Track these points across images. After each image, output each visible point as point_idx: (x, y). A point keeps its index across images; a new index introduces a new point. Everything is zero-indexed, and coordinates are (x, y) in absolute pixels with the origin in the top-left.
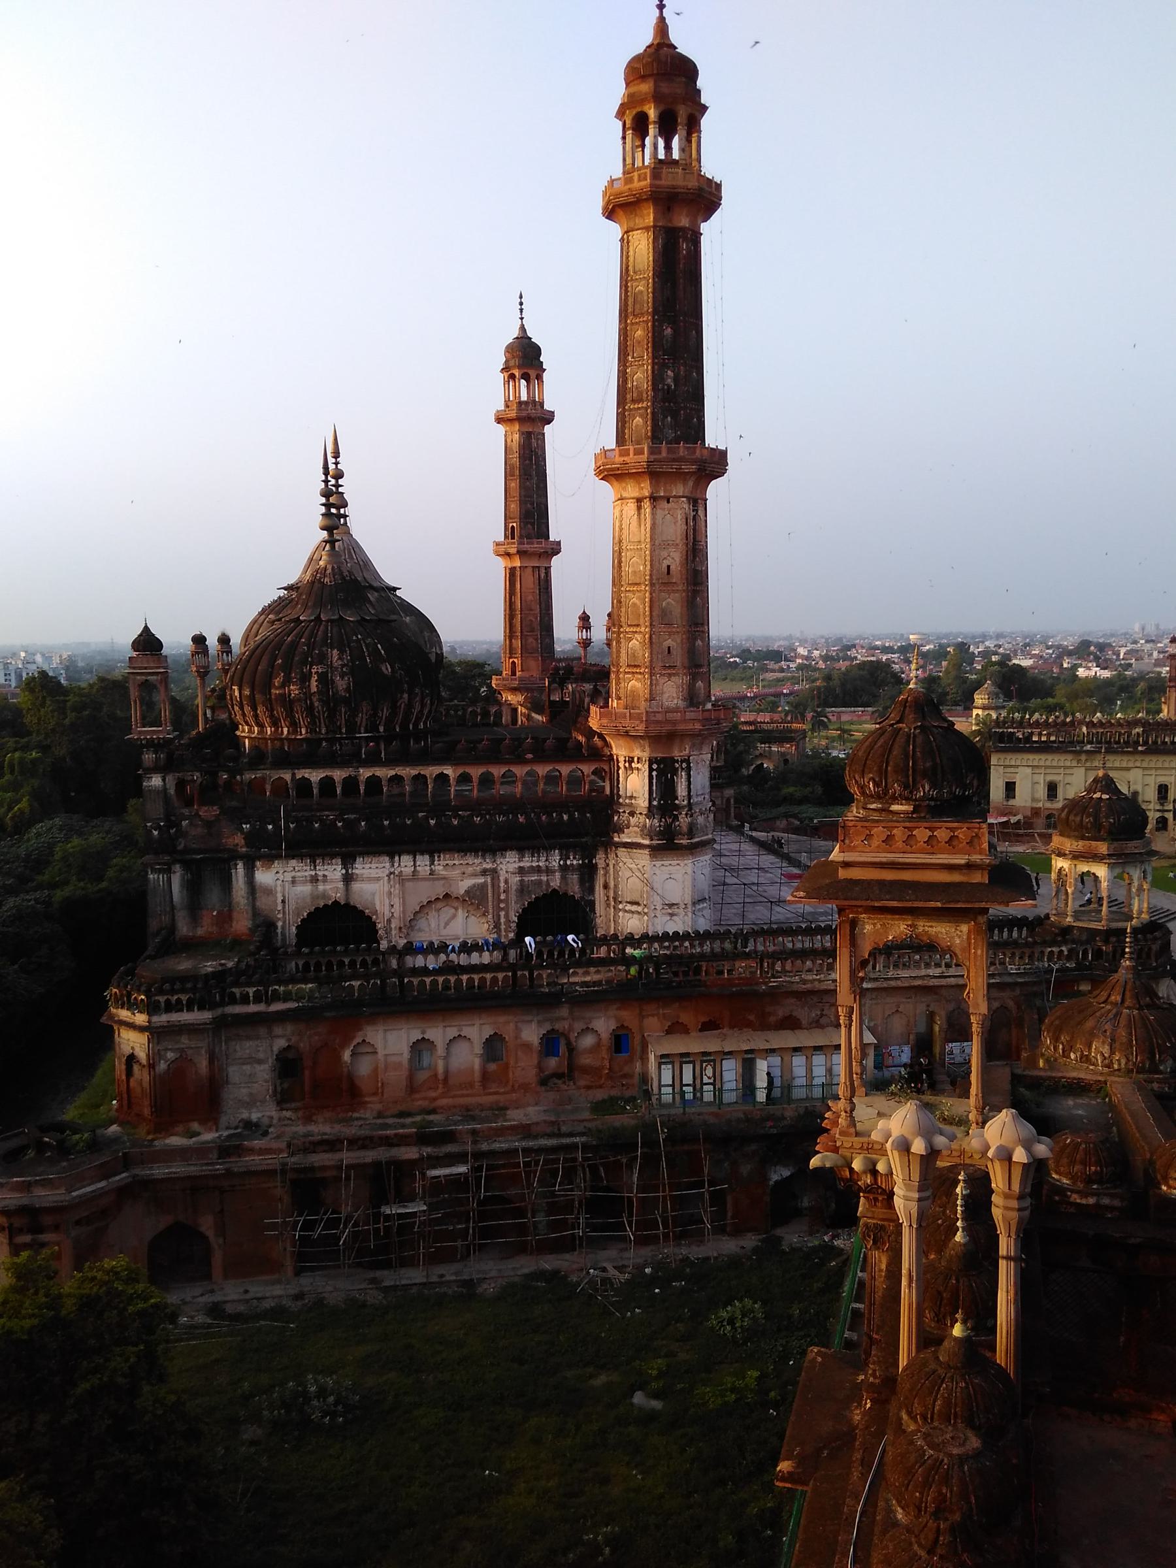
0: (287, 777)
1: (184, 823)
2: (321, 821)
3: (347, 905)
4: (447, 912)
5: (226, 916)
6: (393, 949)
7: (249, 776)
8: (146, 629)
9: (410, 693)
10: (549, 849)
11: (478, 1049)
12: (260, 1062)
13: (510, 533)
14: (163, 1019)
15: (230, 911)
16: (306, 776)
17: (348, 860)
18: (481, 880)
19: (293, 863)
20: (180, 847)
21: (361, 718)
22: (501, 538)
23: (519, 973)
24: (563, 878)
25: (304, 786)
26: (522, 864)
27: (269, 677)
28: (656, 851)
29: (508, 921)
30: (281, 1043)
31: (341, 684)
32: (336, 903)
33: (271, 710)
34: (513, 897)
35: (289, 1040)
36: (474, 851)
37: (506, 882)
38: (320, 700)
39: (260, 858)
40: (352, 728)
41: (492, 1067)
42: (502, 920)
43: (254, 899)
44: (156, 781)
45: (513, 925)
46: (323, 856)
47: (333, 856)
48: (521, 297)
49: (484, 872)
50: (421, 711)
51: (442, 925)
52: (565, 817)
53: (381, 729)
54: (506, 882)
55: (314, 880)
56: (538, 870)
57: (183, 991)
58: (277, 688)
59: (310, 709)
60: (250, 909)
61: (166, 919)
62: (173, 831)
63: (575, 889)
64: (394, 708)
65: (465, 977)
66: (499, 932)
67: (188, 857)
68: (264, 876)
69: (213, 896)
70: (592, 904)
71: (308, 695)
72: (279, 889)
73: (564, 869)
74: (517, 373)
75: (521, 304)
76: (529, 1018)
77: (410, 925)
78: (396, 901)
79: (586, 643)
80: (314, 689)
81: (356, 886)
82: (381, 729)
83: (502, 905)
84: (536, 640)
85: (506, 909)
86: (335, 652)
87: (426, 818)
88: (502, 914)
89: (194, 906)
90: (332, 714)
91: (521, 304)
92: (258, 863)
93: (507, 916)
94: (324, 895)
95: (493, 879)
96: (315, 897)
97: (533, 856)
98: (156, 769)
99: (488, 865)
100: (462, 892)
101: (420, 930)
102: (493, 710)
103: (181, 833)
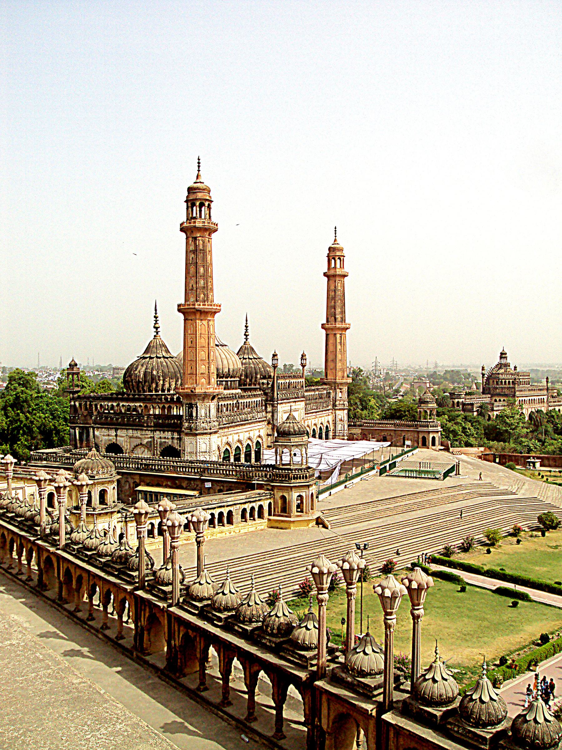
0: (103, 404)
4: (143, 449)
9: (164, 380)
10: (168, 431)
17: (116, 430)
18: (150, 440)
22: (325, 322)
24: (172, 442)
28: (187, 434)
47: (112, 428)
48: (335, 228)
50: (170, 386)
52: (172, 421)
56: (165, 438)
73: (173, 438)
75: (335, 231)
81: (118, 438)
85: (157, 450)
91: (335, 231)
99: (152, 436)
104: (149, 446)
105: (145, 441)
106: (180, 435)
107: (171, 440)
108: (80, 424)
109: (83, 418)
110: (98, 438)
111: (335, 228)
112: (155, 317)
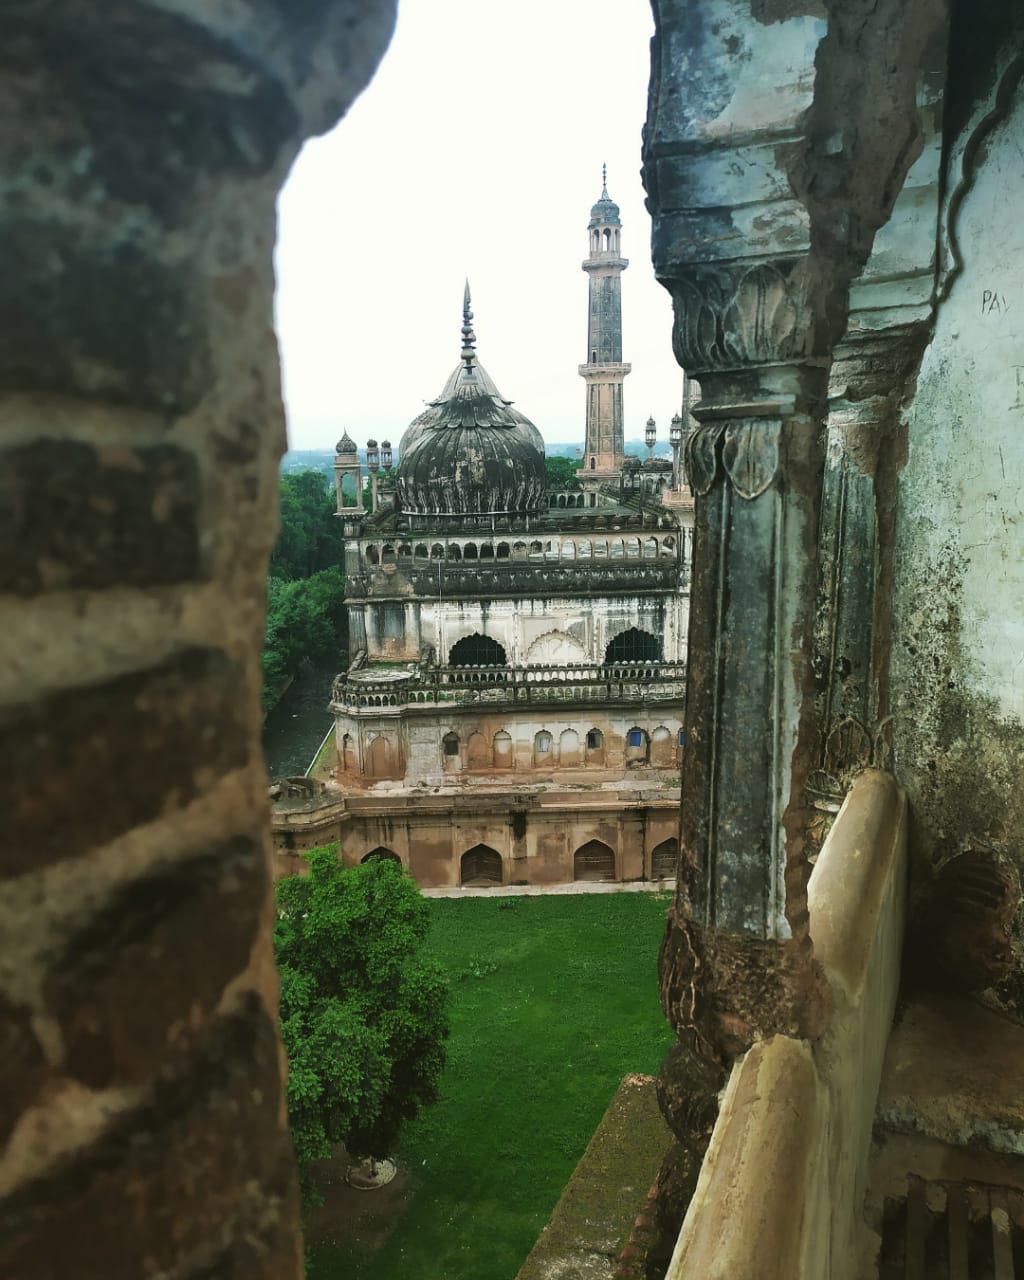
0: (443, 543)
1: (373, 576)
2: (466, 575)
3: (484, 636)
4: (555, 642)
5: (401, 643)
6: (519, 668)
7: (416, 543)
8: (345, 438)
9: (527, 480)
10: (630, 597)
11: (583, 739)
12: (432, 742)
13: (593, 358)
14: (367, 710)
15: (404, 639)
16: (456, 542)
17: (485, 604)
18: (580, 620)
19: (447, 605)
20: (370, 593)
21: (493, 500)
22: (584, 361)
23: (612, 686)
24: (641, 619)
25: (455, 549)
26: (610, 608)
27: (429, 469)
29: (599, 650)
30: (446, 730)
31: (478, 473)
32: (477, 634)
33: (427, 495)
34: (604, 633)
35: (451, 727)
36: (576, 598)
37: (598, 621)
38: (462, 487)
39: (424, 601)
40: (485, 507)
41: (591, 751)
42: (595, 650)
43: (420, 630)
44: (353, 546)
45: (604, 654)
46: (468, 601)
47: (474, 601)
48: (604, 167)
49: (583, 614)
51: (551, 651)
52: (643, 574)
53: (506, 508)
54: (598, 621)
55: (462, 618)
56: (623, 613)
57: (380, 691)
58: (432, 478)
59: (456, 494)
60: (418, 638)
61: (361, 644)
62: (365, 582)
63: (648, 627)
64: (515, 495)
65: (573, 688)
66: (592, 658)
67: (375, 600)
68: (429, 614)
69: (392, 627)
70: (662, 638)
71: (454, 484)
72: (437, 624)
73: (641, 612)
74: (601, 230)
76: (619, 718)
77: (529, 651)
78: (519, 634)
79: (650, 444)
80: (458, 479)
81: (490, 623)
82: (506, 508)
83: (595, 638)
84: (611, 441)
85: (597, 641)
86: (473, 451)
87: (541, 574)
88: (595, 644)
89: (380, 636)
90: (472, 496)
91: (604, 172)
92: (423, 605)
93: (598, 646)
94: (468, 629)
95: (588, 619)
96: (461, 631)
97: (618, 602)
98: (353, 537)
100: (566, 628)
101: (535, 655)
102: (576, 495)
103: (370, 583)
104: (575, 634)
105: (565, 625)
106: (661, 604)
107: (637, 616)
108: (374, 595)
109: (383, 581)
110: (430, 626)
111: (604, 167)
112: (463, 332)
